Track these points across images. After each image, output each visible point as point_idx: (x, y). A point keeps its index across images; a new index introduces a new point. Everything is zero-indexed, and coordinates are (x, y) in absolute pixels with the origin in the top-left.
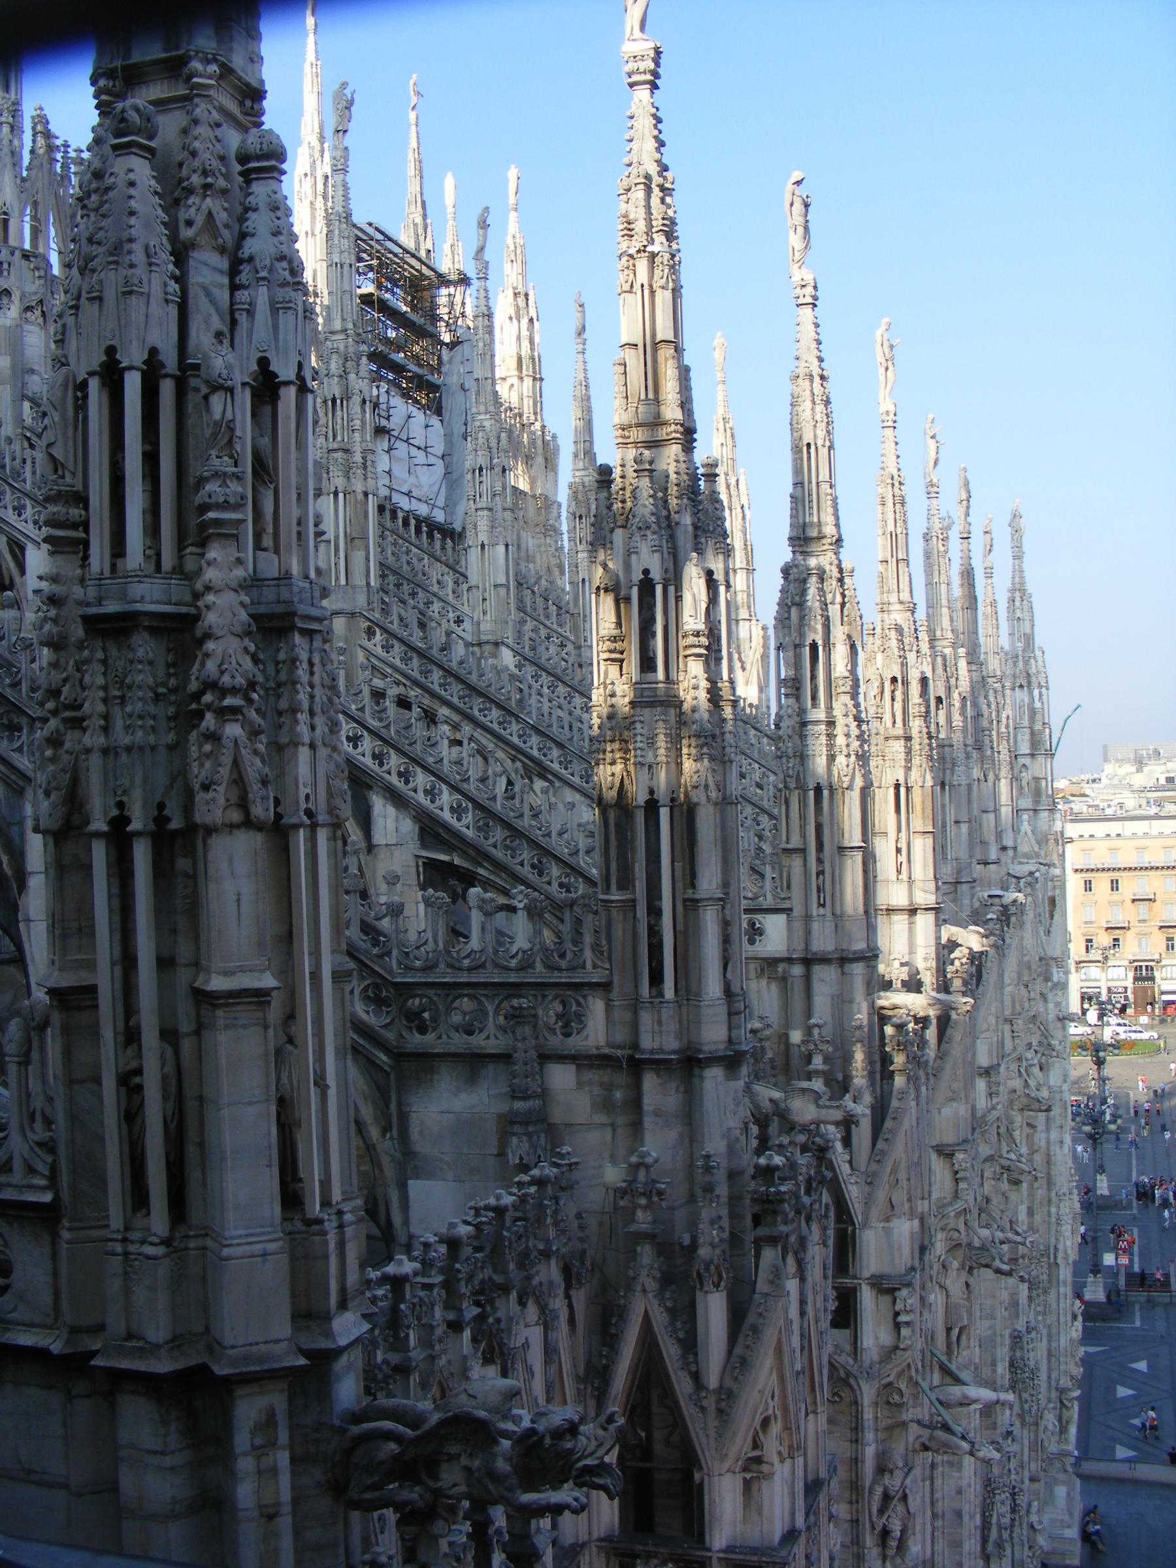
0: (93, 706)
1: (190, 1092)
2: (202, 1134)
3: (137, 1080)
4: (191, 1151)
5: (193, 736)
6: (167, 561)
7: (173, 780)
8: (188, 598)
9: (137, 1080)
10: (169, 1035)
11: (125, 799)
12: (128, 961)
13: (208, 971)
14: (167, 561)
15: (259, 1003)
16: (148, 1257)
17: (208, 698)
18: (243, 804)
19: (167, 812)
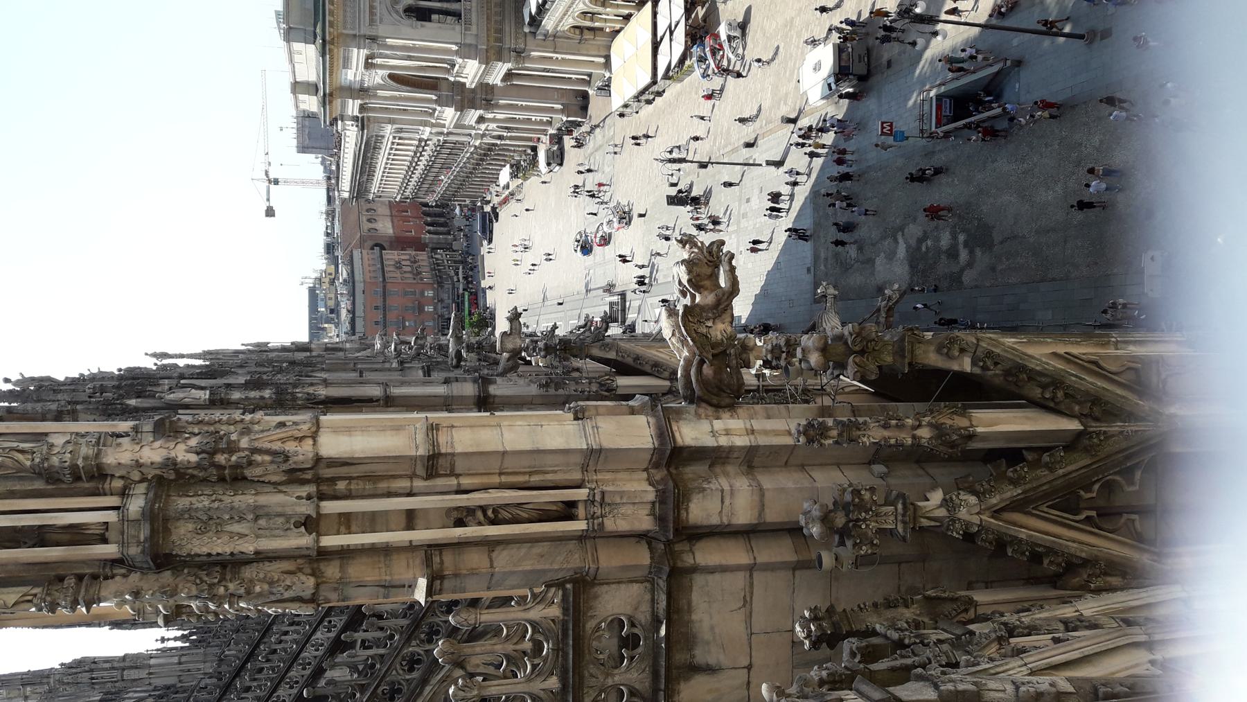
0: (220, 546)
1: (496, 480)
2: (524, 473)
3: (490, 513)
4: (535, 479)
5: (248, 473)
6: (114, 501)
7: (280, 492)
8: (145, 485)
9: (490, 513)
10: (461, 491)
11: (292, 521)
12: (410, 519)
13: (413, 459)
14: (114, 501)
15: (438, 430)
16: (603, 498)
17: (221, 458)
18: (301, 439)
19: (304, 494)
